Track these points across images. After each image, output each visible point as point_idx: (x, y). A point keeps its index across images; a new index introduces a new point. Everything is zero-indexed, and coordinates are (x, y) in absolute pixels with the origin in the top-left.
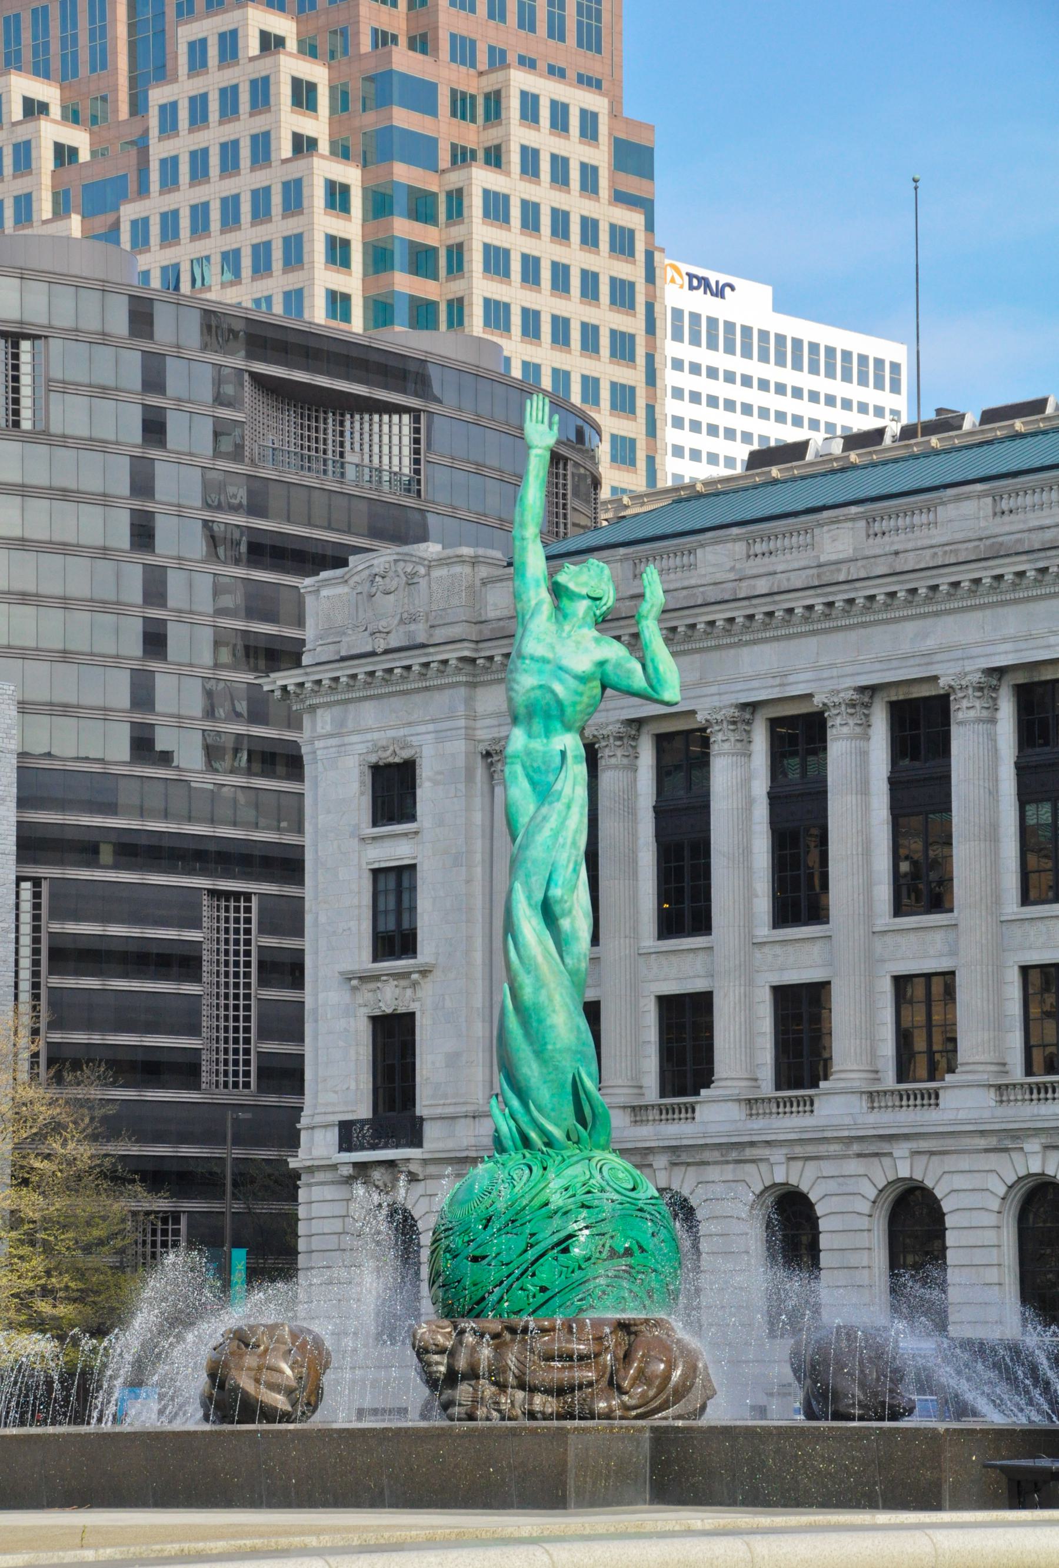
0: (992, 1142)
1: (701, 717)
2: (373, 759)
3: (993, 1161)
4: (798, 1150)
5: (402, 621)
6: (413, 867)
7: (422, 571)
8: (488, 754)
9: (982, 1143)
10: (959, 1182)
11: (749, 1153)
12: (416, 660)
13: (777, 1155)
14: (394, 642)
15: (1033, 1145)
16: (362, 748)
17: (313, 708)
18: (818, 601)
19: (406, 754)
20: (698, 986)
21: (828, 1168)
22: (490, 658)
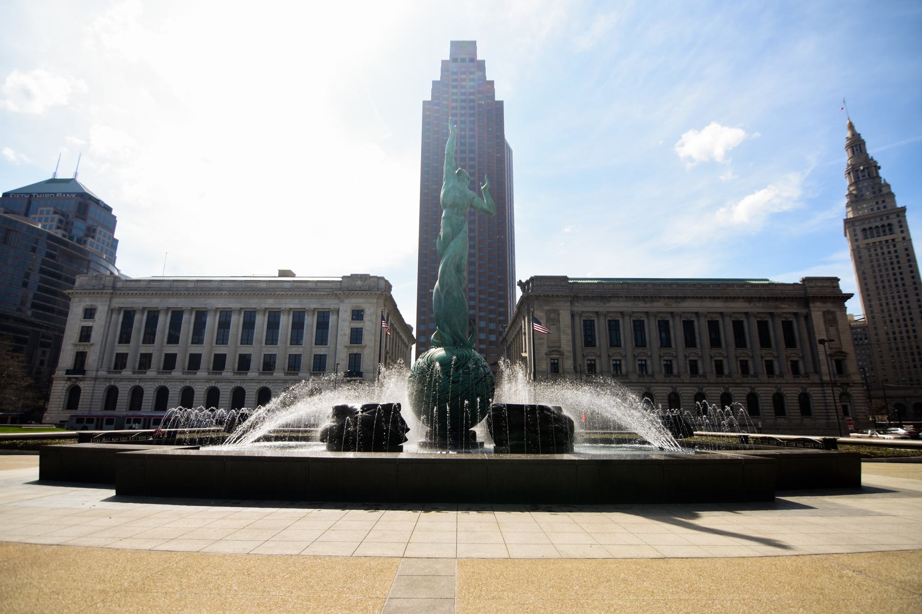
0: (205, 381)
1: (159, 309)
2: (86, 307)
3: (205, 384)
4: (167, 380)
5: (98, 285)
6: (92, 327)
7: (104, 277)
8: (112, 310)
9: (203, 381)
10: (199, 387)
11: (156, 380)
12: (100, 291)
13: (163, 381)
14: (95, 288)
15: (213, 382)
16: (84, 305)
17: (75, 297)
18: (187, 293)
19: (94, 307)
20: (150, 352)
21: (173, 384)
22: (117, 294)
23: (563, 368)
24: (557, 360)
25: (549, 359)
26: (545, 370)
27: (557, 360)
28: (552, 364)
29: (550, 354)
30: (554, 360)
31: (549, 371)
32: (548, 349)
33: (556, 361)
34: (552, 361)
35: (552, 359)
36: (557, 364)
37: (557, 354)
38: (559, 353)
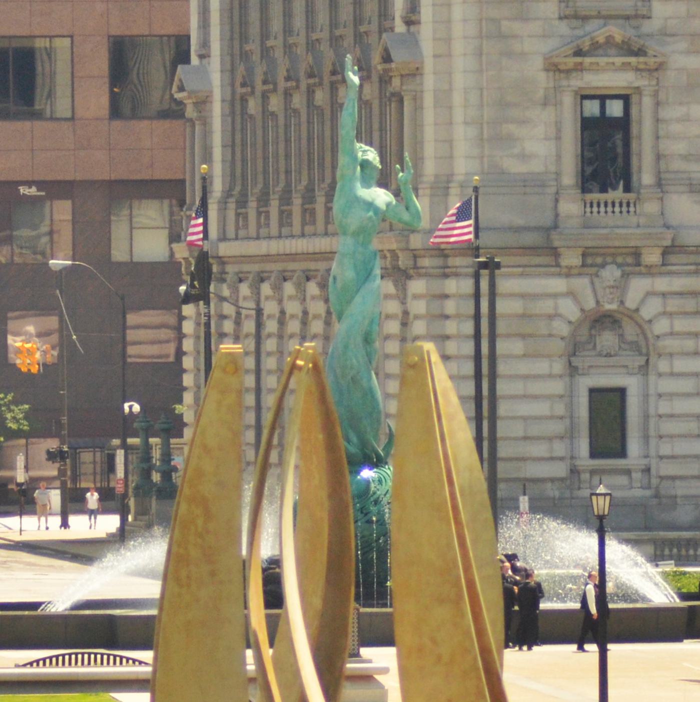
23: (658, 157)
24: (626, 99)
25: (568, 100)
26: (536, 166)
27: (626, 99)
28: (587, 124)
29: (579, 68)
30: (603, 99)
31: (569, 178)
32: (563, 28)
33: (615, 109)
34: (592, 108)
35: (584, 97)
36: (624, 124)
37: (626, 66)
38: (633, 60)
